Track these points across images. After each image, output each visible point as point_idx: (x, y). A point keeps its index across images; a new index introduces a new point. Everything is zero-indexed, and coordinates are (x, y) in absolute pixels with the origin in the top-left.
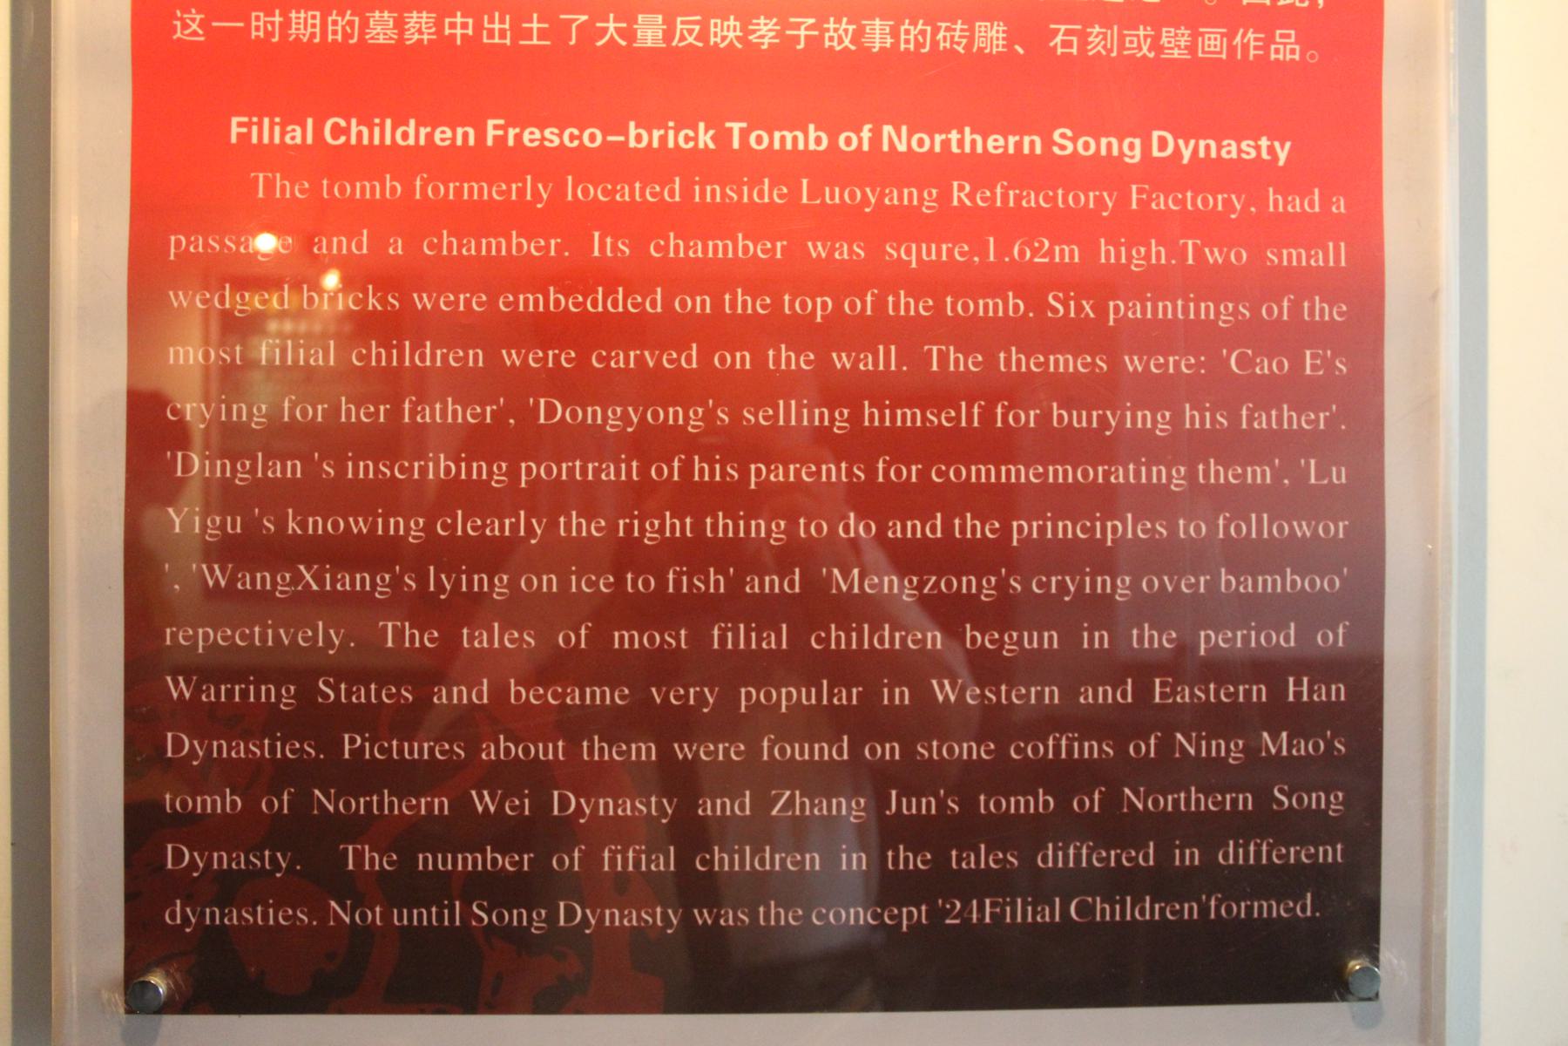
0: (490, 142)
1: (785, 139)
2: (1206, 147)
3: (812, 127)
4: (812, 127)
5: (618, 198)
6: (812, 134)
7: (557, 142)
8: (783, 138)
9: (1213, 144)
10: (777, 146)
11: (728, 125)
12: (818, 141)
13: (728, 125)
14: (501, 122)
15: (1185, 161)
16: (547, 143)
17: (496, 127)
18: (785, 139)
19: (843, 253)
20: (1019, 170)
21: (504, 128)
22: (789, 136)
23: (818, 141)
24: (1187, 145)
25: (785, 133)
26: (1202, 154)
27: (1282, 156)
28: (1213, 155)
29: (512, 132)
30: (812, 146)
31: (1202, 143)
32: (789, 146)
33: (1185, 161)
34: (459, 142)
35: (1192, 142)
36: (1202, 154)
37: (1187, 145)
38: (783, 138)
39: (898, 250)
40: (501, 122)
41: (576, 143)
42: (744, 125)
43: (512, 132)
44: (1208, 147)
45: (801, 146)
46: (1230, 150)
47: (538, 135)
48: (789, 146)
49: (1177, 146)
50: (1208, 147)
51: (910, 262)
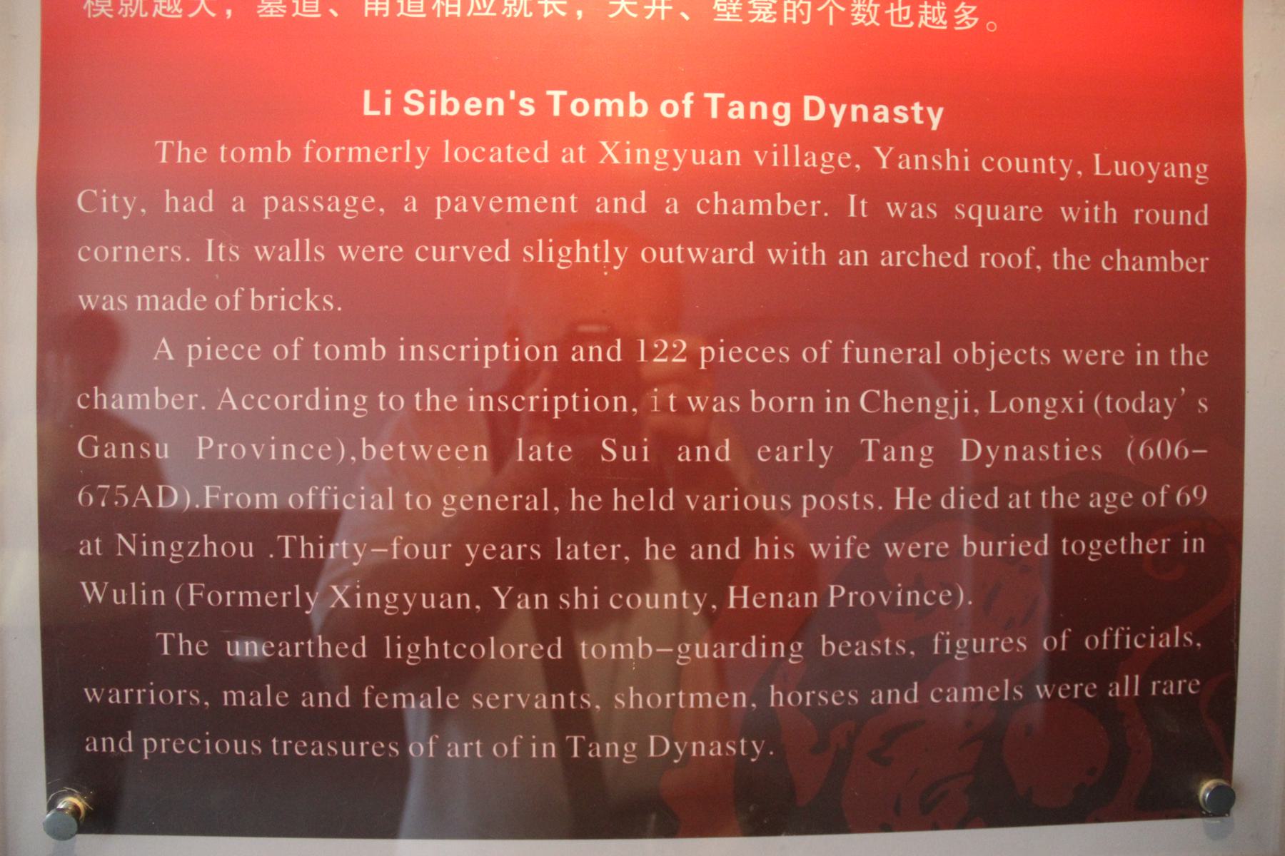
1: (606, 106)
2: (858, 111)
3: (632, 95)
4: (632, 95)
5: (491, 159)
6: (633, 102)
8: (603, 106)
9: (865, 109)
10: (597, 113)
12: (639, 108)
15: (837, 125)
18: (606, 106)
19: (918, 213)
20: (509, 128)
22: (609, 103)
23: (639, 108)
26: (854, 118)
27: (935, 122)
28: (865, 119)
30: (633, 113)
31: (854, 108)
32: (609, 113)
33: (837, 125)
34: (489, 112)
35: (843, 107)
36: (854, 118)
37: (838, 109)
38: (603, 106)
39: (966, 211)
44: (860, 112)
46: (882, 115)
48: (609, 113)
49: (828, 109)
50: (860, 112)
51: (976, 222)
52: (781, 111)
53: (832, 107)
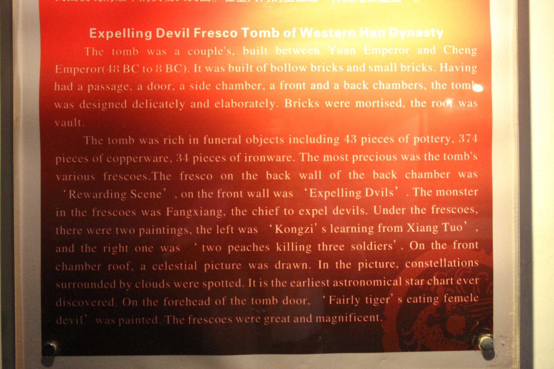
0: (195, 36)
7: (220, 36)
11: (242, 29)
13: (242, 29)
14: (199, 29)
16: (217, 36)
17: (198, 31)
21: (201, 31)
24: (178, 33)
25: (264, 31)
29: (203, 32)
35: (180, 32)
40: (199, 29)
41: (227, 36)
42: (248, 29)
43: (203, 32)
45: (269, 36)
47: (213, 33)
52: (148, 34)
53: (176, 32)
